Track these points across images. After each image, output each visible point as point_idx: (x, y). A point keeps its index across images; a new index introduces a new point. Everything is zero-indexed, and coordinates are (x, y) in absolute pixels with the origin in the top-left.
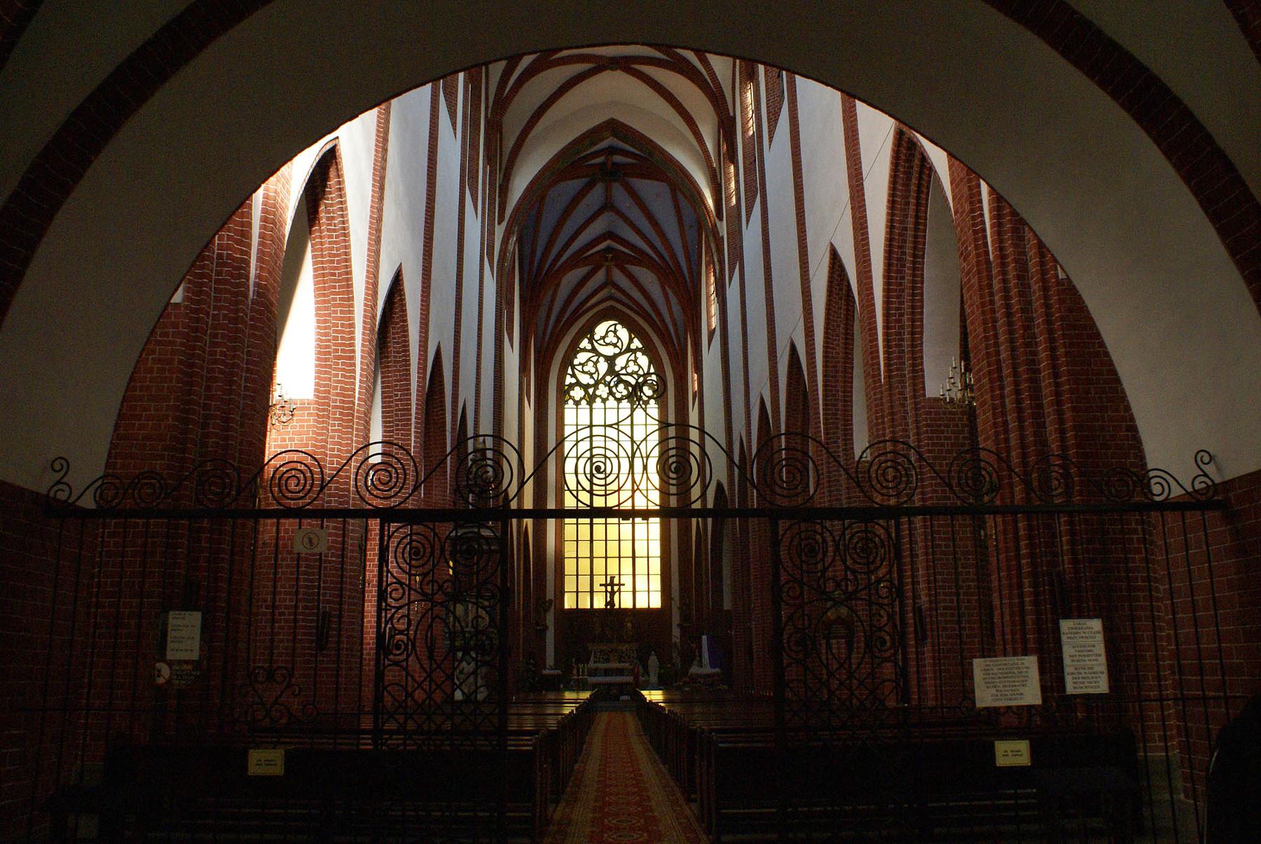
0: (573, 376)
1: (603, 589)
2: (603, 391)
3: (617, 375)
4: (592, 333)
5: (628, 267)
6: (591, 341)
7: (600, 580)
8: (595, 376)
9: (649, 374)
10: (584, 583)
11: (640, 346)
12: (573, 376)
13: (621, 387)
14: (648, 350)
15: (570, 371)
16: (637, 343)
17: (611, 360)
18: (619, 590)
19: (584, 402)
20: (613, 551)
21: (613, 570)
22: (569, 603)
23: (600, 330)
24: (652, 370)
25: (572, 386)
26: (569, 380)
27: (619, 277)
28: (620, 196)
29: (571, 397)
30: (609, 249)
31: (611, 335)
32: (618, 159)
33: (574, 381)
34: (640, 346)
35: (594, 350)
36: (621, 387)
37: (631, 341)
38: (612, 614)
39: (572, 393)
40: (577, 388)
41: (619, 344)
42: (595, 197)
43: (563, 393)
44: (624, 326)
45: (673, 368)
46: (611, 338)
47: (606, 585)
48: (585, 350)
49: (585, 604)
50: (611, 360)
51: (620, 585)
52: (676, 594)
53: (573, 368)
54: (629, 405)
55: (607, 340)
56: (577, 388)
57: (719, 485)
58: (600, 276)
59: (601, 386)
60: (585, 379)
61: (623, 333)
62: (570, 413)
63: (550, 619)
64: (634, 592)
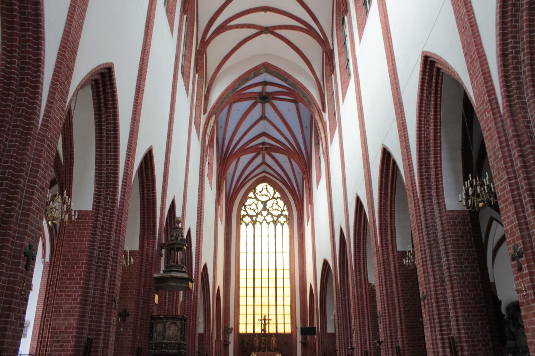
0: (245, 211)
1: (260, 322)
2: (260, 218)
3: (268, 210)
4: (254, 189)
5: (274, 154)
6: (254, 193)
7: (258, 317)
9: (284, 210)
11: (279, 196)
12: (245, 211)
15: (243, 208)
16: (278, 195)
17: (264, 203)
18: (269, 323)
19: (250, 224)
20: (265, 302)
21: (265, 312)
22: (242, 330)
23: (259, 188)
24: (285, 208)
25: (244, 216)
26: (243, 213)
27: (269, 160)
28: (270, 112)
30: (263, 143)
31: (264, 190)
32: (270, 89)
33: (245, 213)
35: (256, 198)
36: (270, 216)
37: (275, 193)
38: (265, 336)
39: (244, 219)
40: (247, 217)
41: (269, 195)
42: (257, 112)
43: (240, 220)
44: (271, 186)
45: (297, 207)
46: (265, 192)
47: (261, 320)
48: (251, 198)
49: (250, 330)
51: (269, 320)
52: (299, 325)
53: (245, 206)
54: (274, 226)
55: (263, 193)
56: (247, 217)
57: (326, 263)
58: (259, 160)
59: (259, 216)
60: (251, 213)
61: (271, 189)
63: (231, 338)
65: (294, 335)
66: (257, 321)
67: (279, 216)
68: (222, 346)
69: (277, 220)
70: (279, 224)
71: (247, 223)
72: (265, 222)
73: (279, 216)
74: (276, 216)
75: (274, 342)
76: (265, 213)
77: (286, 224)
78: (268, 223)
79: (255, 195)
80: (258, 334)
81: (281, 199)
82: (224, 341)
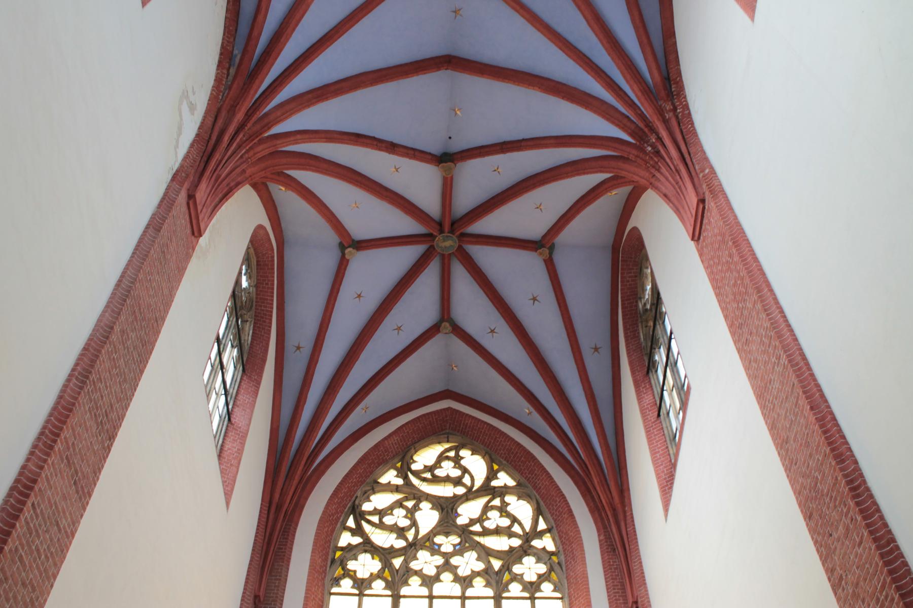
2: (426, 562)
6: (404, 472)
8: (410, 535)
12: (358, 531)
19: (378, 586)
23: (425, 457)
24: (542, 525)
25: (351, 551)
29: (348, 574)
33: (357, 540)
34: (511, 483)
37: (492, 475)
41: (467, 480)
50: (447, 507)
53: (361, 517)
59: (423, 555)
61: (476, 465)
67: (512, 557)
69: (507, 568)
70: (515, 589)
71: (362, 574)
72: (447, 577)
73: (512, 557)
74: (498, 554)
76: (447, 543)
78: (466, 582)
79: (406, 478)
81: (521, 492)
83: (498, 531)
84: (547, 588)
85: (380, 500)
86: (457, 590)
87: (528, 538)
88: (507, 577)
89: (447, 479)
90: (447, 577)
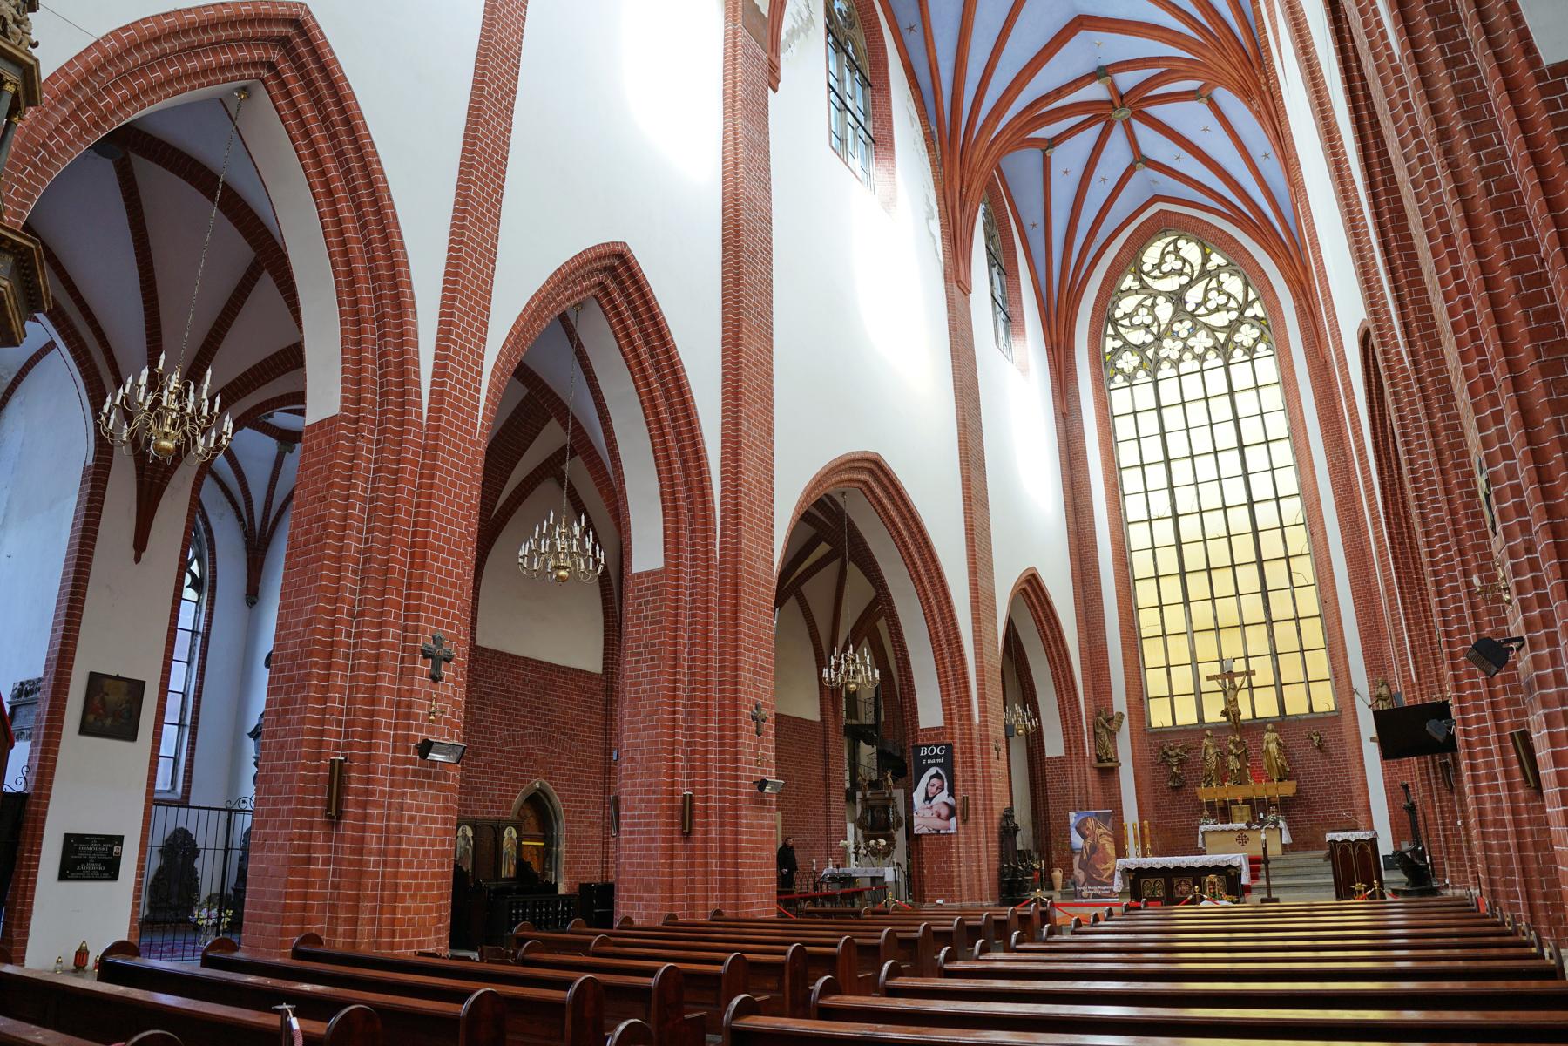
1: (1215, 685)
2: (1170, 348)
3: (1193, 315)
6: (1139, 273)
8: (1154, 329)
9: (1248, 304)
10: (1182, 680)
11: (1223, 262)
12: (1117, 336)
13: (1202, 334)
14: (1241, 263)
15: (1110, 331)
16: (1217, 260)
19: (1141, 374)
21: (1232, 647)
23: (1151, 256)
26: (1110, 344)
33: (1118, 343)
34: (1223, 262)
35: (1144, 287)
36: (1202, 334)
37: (1206, 258)
38: (1241, 731)
41: (1187, 269)
43: (1103, 366)
45: (1288, 281)
46: (1172, 263)
49: (1187, 716)
50: (1177, 298)
53: (1115, 323)
55: (1166, 268)
56: (1127, 356)
59: (1167, 342)
60: (1136, 337)
61: (1191, 251)
62: (1120, 400)
63: (1124, 749)
64: (1279, 685)
65: (1346, 720)
66: (1206, 685)
67: (1232, 327)
68: (1091, 775)
69: (1229, 339)
70: (1238, 354)
71: (1128, 369)
73: (1232, 327)
75: (1273, 747)
76: (1182, 328)
77: (1261, 347)
78: (1202, 358)
80: (1216, 728)
82: (1099, 759)
83: (1217, 309)
84: (1261, 347)
85: (1127, 305)
86: (1196, 366)
87: (1242, 309)
88: (1231, 346)
89: (1172, 272)
90: (1187, 356)
